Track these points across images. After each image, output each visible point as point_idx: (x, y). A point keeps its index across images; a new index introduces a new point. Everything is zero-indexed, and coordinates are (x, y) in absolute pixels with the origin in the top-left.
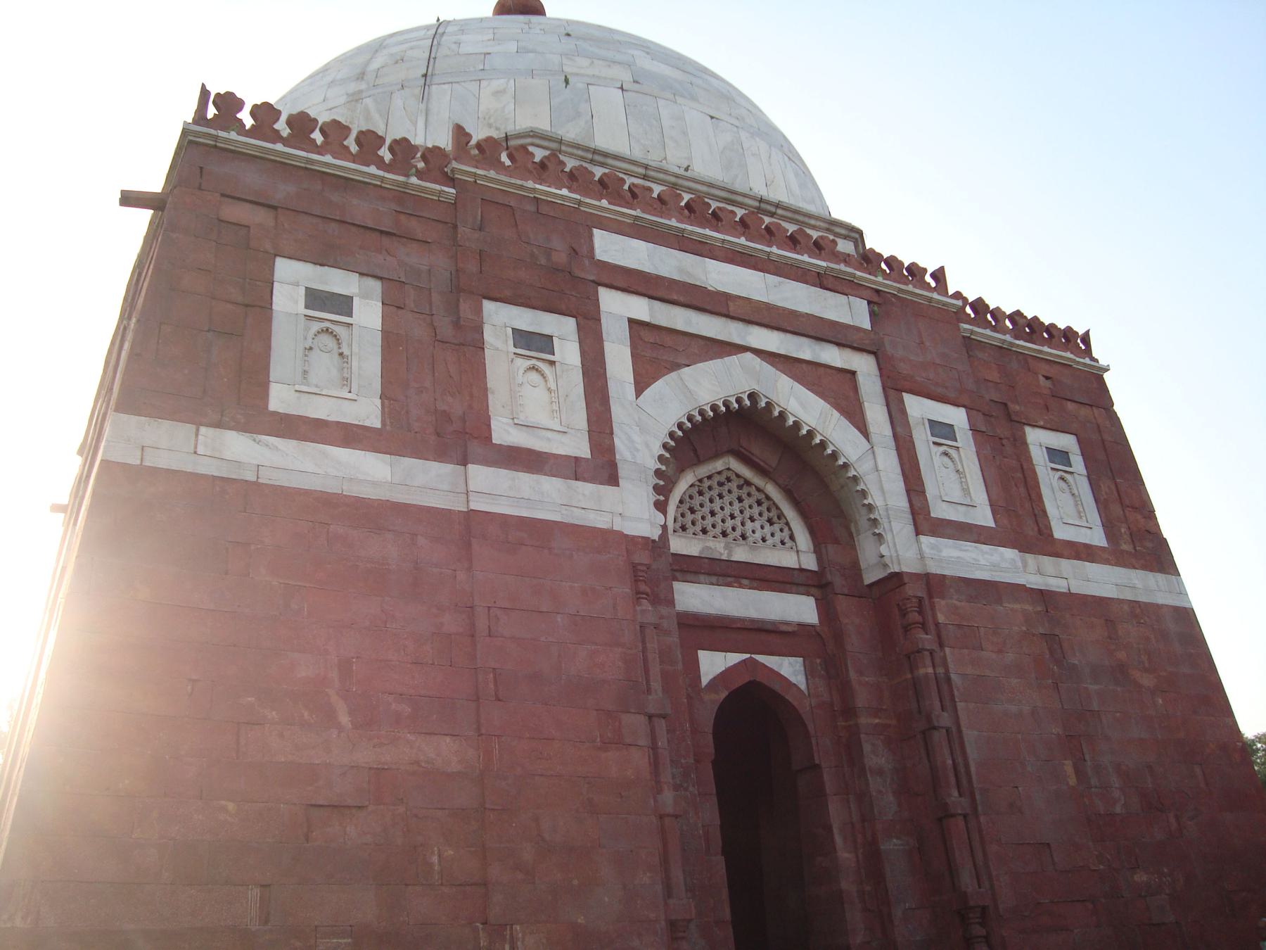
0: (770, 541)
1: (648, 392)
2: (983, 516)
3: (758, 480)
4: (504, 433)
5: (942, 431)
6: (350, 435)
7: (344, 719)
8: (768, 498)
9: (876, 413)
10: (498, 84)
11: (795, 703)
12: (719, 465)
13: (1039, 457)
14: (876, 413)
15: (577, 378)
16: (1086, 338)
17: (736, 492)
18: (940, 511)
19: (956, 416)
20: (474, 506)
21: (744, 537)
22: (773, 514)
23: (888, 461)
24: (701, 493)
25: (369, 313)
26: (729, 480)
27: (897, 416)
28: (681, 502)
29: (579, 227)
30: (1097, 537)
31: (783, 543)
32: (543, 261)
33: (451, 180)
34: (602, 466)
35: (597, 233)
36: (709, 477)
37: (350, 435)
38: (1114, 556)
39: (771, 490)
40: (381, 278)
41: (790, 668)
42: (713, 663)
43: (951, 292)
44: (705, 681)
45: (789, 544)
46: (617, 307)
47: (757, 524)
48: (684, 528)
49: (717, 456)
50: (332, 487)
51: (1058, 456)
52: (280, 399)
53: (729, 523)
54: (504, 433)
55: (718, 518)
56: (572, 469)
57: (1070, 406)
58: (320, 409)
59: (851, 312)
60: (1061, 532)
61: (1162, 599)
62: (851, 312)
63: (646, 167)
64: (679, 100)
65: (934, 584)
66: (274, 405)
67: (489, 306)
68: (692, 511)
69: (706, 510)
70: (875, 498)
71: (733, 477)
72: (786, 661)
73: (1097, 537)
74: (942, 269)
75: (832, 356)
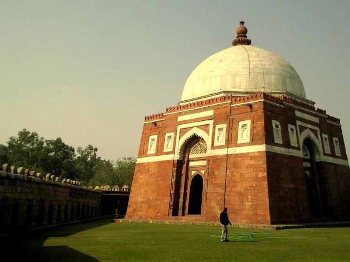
2: (329, 153)
5: (326, 139)
13: (334, 142)
14: (319, 137)
16: (339, 120)
18: (326, 152)
20: (291, 154)
23: (321, 144)
25: (279, 126)
29: (293, 110)
30: (340, 155)
33: (283, 105)
35: (296, 111)
39: (306, 147)
41: (308, 173)
52: (276, 141)
54: (292, 145)
59: (316, 120)
60: (337, 154)
61: (347, 165)
62: (316, 120)
65: (326, 163)
67: (288, 125)
70: (320, 150)
73: (340, 155)
75: (316, 128)
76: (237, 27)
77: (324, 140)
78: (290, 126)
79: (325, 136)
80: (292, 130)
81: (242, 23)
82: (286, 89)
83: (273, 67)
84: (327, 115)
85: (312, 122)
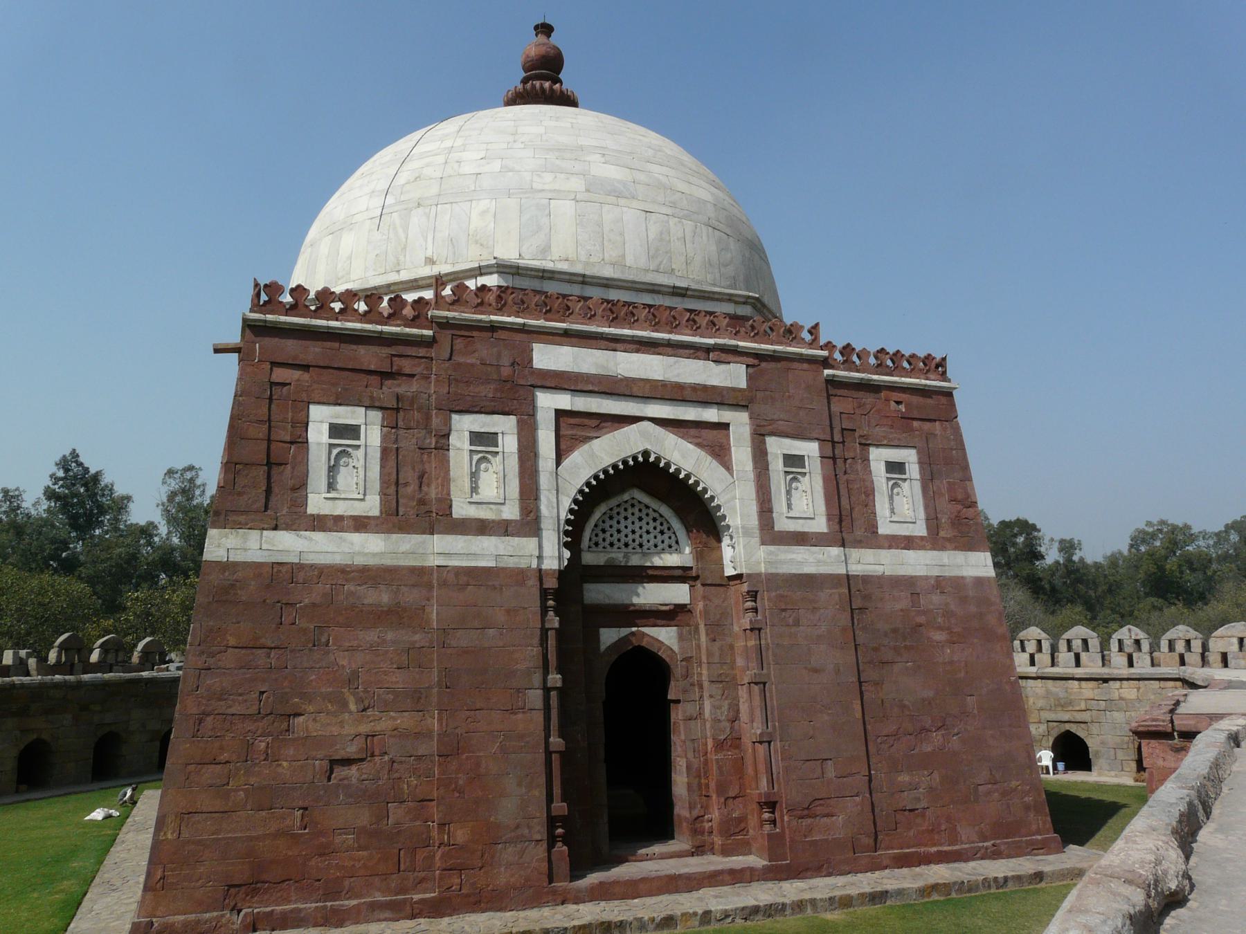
0: (660, 546)
1: (566, 463)
3: (654, 504)
4: (461, 509)
5: (793, 461)
6: (360, 524)
7: (353, 707)
8: (661, 516)
9: (741, 454)
10: (484, 204)
11: (667, 660)
12: (626, 497)
14: (741, 454)
15: (513, 464)
16: (942, 363)
17: (637, 514)
18: (782, 524)
19: (810, 449)
21: (641, 545)
22: (665, 526)
24: (611, 518)
25: (373, 435)
26: (633, 506)
27: (760, 456)
28: (596, 526)
31: (670, 547)
32: (495, 377)
34: (529, 524)
36: (618, 506)
37: (360, 524)
38: (934, 540)
39: (665, 511)
40: (381, 408)
42: (609, 636)
43: (822, 342)
44: (603, 648)
45: (675, 546)
46: (548, 402)
47: (652, 535)
48: (597, 544)
49: (623, 491)
50: (347, 561)
51: (895, 468)
53: (631, 537)
55: (622, 535)
56: (503, 528)
57: (916, 424)
58: (340, 509)
59: (733, 376)
62: (733, 376)
63: (584, 276)
64: (622, 201)
66: (312, 509)
68: (604, 531)
69: (614, 529)
71: (635, 502)
72: (664, 630)
74: (817, 324)
75: (711, 415)
76: (532, 45)
77: (777, 466)
78: (464, 425)
79: (777, 447)
80: (483, 439)
81: (545, 29)
82: (546, 249)
83: (496, 166)
84: (829, 346)
85: (680, 387)
